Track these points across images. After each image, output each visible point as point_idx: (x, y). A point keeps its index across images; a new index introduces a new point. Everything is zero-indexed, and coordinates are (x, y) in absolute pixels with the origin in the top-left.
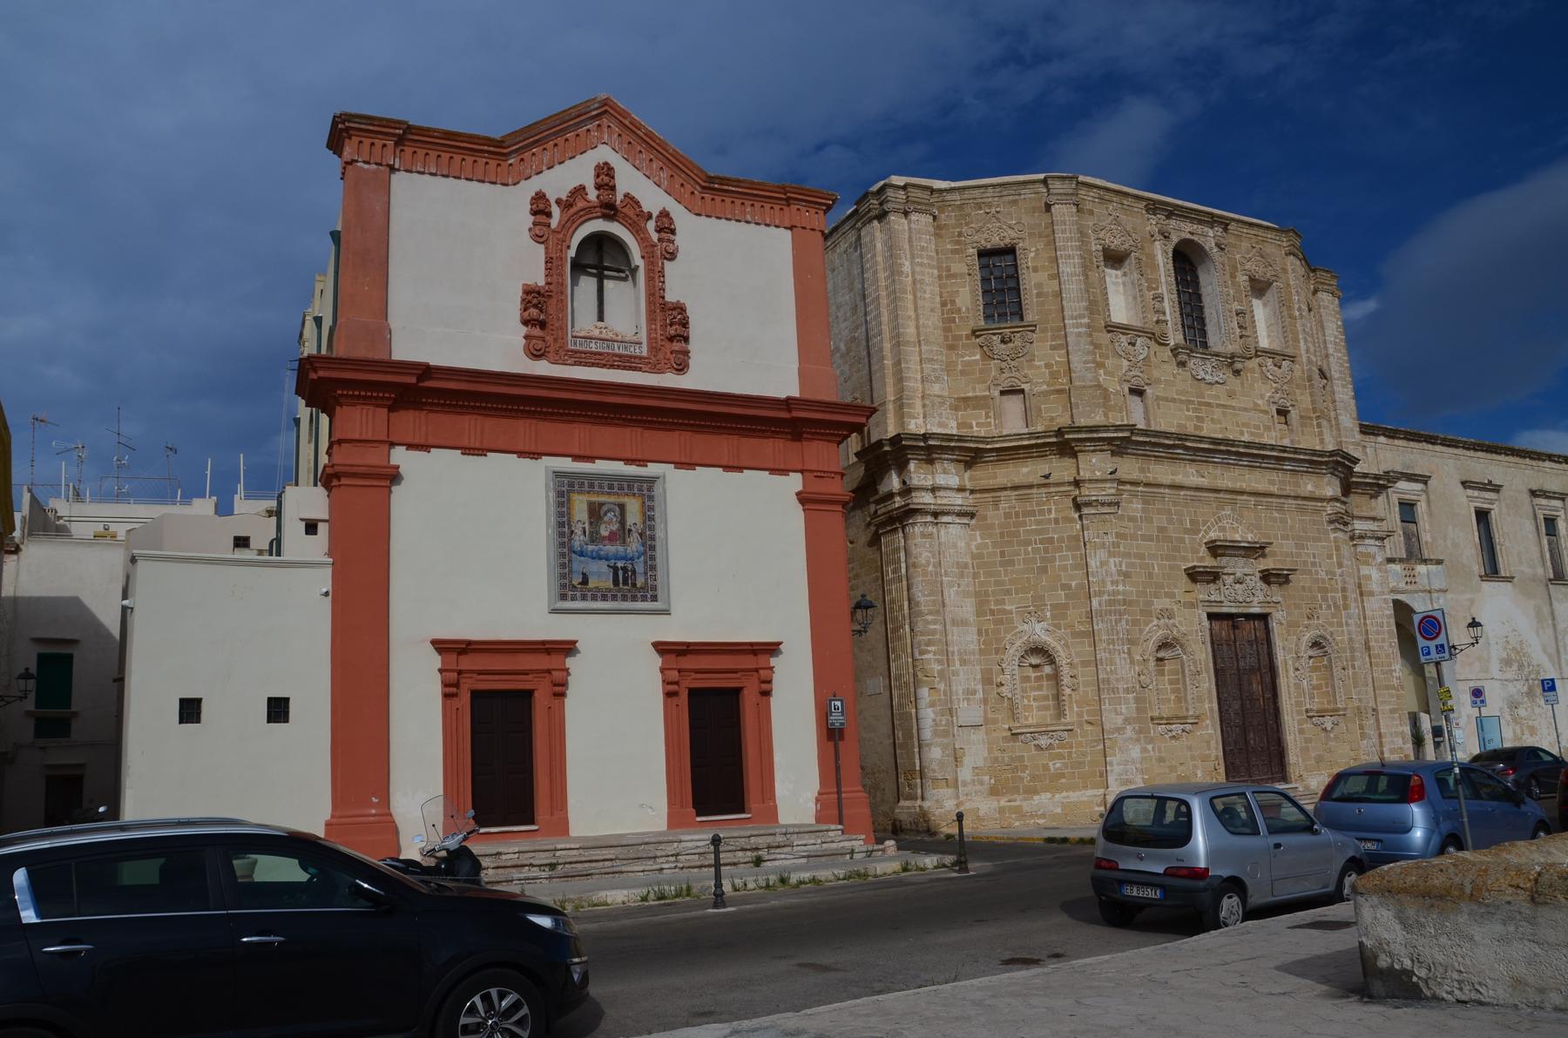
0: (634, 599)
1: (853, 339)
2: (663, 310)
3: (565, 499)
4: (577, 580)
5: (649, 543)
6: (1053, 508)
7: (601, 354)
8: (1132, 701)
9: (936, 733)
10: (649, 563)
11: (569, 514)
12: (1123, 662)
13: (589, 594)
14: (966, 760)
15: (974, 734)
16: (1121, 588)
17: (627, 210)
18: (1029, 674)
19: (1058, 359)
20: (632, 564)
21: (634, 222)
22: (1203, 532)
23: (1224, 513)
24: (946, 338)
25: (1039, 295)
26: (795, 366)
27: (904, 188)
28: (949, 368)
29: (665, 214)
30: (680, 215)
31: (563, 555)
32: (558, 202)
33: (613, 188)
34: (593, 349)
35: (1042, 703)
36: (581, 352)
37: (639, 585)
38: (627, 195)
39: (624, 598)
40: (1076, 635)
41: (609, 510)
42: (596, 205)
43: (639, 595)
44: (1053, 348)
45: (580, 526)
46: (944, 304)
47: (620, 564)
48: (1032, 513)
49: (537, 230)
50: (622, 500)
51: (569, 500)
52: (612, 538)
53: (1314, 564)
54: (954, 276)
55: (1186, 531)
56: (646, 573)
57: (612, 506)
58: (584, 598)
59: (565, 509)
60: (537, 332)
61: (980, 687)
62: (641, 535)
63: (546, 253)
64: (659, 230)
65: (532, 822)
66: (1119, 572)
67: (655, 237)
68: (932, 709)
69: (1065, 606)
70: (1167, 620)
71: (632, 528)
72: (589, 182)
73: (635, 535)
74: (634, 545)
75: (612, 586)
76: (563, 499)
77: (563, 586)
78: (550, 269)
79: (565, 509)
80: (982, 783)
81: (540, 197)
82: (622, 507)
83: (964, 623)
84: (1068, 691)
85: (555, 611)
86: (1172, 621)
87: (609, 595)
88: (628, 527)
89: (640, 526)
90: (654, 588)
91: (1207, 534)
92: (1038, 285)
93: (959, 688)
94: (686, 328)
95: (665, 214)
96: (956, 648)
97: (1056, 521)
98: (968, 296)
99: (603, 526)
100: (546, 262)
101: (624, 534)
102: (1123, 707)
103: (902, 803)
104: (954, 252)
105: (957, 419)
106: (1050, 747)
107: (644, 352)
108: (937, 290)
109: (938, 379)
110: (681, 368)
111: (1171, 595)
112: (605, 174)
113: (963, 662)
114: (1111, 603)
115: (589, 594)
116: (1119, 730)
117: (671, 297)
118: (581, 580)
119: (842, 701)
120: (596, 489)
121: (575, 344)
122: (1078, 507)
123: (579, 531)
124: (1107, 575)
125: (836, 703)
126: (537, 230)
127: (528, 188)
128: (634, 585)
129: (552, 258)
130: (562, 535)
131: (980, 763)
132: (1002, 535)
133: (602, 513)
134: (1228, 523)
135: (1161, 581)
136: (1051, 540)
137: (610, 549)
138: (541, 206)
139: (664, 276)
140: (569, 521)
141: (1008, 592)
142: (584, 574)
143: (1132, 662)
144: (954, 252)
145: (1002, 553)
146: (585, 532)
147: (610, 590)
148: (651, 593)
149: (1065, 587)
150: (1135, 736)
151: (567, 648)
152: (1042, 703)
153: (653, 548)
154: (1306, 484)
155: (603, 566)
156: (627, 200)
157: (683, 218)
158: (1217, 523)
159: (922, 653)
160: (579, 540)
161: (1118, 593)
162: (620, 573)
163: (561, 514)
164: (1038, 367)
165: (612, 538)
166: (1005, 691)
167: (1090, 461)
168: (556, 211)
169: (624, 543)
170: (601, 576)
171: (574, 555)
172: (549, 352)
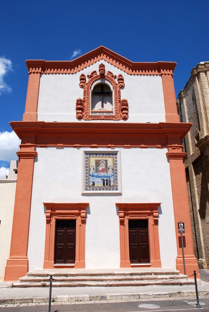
0: (110, 190)
2: (120, 102)
3: (88, 159)
4: (91, 184)
5: (115, 172)
7: (100, 116)
10: (115, 178)
11: (89, 164)
13: (95, 188)
21: (111, 78)
26: (164, 115)
27: (204, 65)
31: (87, 176)
32: (88, 76)
33: (104, 70)
36: (94, 116)
37: (111, 185)
39: (107, 189)
41: (102, 162)
43: (111, 188)
45: (93, 167)
47: (105, 179)
49: (82, 84)
50: (106, 159)
51: (89, 160)
52: (103, 171)
56: (114, 181)
58: (93, 190)
60: (80, 111)
62: (112, 169)
63: (84, 90)
64: (119, 80)
71: (110, 167)
73: (111, 169)
74: (110, 173)
75: (102, 186)
77: (86, 186)
78: (85, 94)
81: (83, 75)
82: (106, 161)
85: (83, 194)
89: (112, 167)
90: (117, 186)
94: (127, 106)
95: (120, 76)
99: (100, 167)
100: (84, 92)
101: (107, 169)
103: (200, 259)
107: (114, 114)
110: (125, 119)
112: (102, 66)
115: (95, 188)
117: (122, 98)
119: (183, 223)
123: (92, 169)
125: (181, 224)
126: (82, 84)
128: (110, 185)
129: (85, 91)
130: (87, 170)
133: (100, 163)
137: (102, 174)
138: (83, 77)
139: (120, 93)
140: (89, 166)
142: (93, 182)
146: (94, 169)
147: (102, 187)
148: (116, 188)
156: (109, 73)
157: (126, 76)
160: (92, 171)
162: (105, 182)
163: (87, 164)
165: (103, 171)
168: (87, 80)
170: (99, 183)
171: (90, 176)
172: (84, 117)
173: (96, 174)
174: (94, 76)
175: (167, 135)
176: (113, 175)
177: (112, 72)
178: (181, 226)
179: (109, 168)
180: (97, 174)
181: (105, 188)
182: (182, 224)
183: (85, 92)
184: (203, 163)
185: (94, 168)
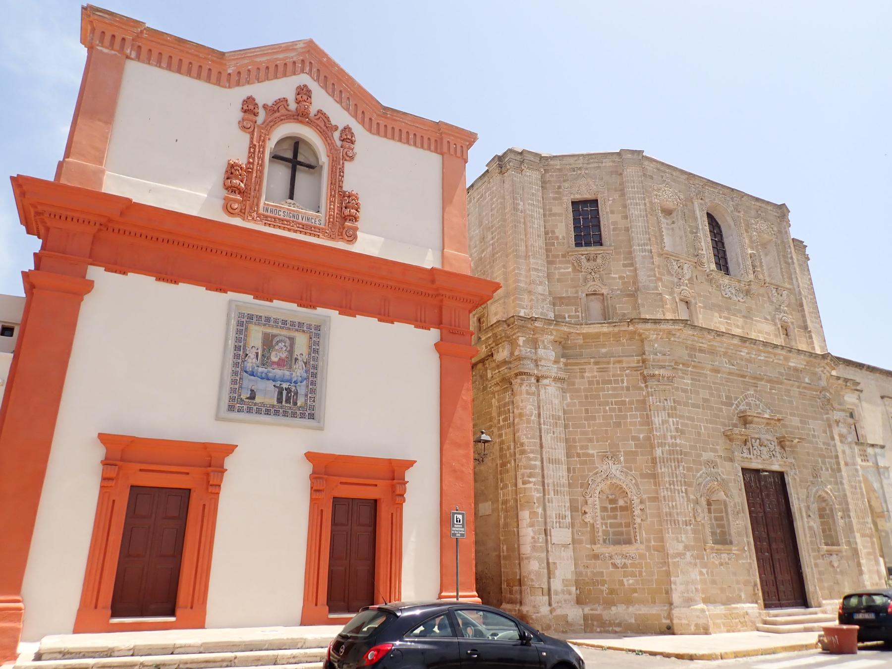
1: (481, 259)
3: (244, 328)
4: (245, 395)
6: (625, 379)
8: (690, 532)
9: (534, 548)
10: (310, 387)
12: (682, 500)
13: (255, 408)
14: (557, 573)
15: (564, 551)
16: (678, 441)
17: (323, 124)
18: (606, 506)
19: (628, 273)
20: (295, 387)
22: (735, 405)
23: (749, 392)
24: (547, 256)
25: (614, 230)
28: (549, 276)
29: (347, 129)
30: (358, 130)
31: (235, 373)
32: (265, 107)
34: (282, 217)
35: (617, 529)
37: (299, 404)
38: (319, 111)
39: (285, 414)
40: (643, 476)
42: (294, 113)
43: (298, 412)
44: (625, 266)
45: (254, 350)
46: (546, 233)
47: (285, 385)
48: (610, 382)
51: (246, 329)
52: (281, 363)
53: (814, 436)
54: (555, 215)
55: (723, 403)
56: (306, 395)
57: (284, 338)
58: (249, 410)
59: (242, 336)
61: (568, 513)
62: (305, 363)
65: (172, 613)
66: (677, 430)
67: (339, 143)
68: (531, 528)
69: (635, 453)
70: (712, 469)
71: (299, 357)
72: (291, 97)
73: (300, 363)
74: (299, 371)
75: (275, 403)
76: (242, 328)
77: (232, 399)
79: (242, 336)
80: (570, 593)
82: (292, 340)
83: (557, 462)
84: (638, 520)
86: (716, 470)
87: (272, 410)
88: (295, 356)
89: (305, 357)
90: (313, 408)
91: (738, 407)
92: (614, 223)
93: (552, 513)
95: (347, 129)
96: (551, 481)
97: (628, 388)
98: (564, 228)
99: (273, 354)
102: (683, 536)
104: (555, 199)
105: (554, 312)
106: (625, 566)
108: (542, 223)
109: (541, 283)
111: (714, 450)
112: (303, 93)
113: (556, 492)
114: (671, 452)
115: (255, 408)
116: (681, 555)
117: (347, 187)
118: (249, 396)
119: (463, 514)
120: (272, 323)
121: (267, 210)
122: (645, 379)
123: (252, 355)
124: (667, 430)
127: (241, 93)
128: (295, 404)
130: (236, 356)
131: (569, 576)
132: (586, 397)
133: (274, 343)
134: (752, 400)
135: (707, 439)
136: (624, 403)
137: (278, 372)
138: (251, 107)
139: (343, 172)
140: (245, 346)
141: (591, 440)
142: (252, 391)
143: (688, 500)
144: (555, 199)
145: (587, 411)
147: (273, 406)
149: (635, 438)
150: (693, 561)
151: (229, 449)
152: (617, 529)
153: (314, 375)
154: (804, 378)
155: (270, 385)
158: (745, 400)
159: (524, 483)
160: (251, 362)
161: (676, 445)
162: (285, 393)
164: (615, 278)
165: (281, 363)
166: (588, 518)
167: (654, 346)
169: (291, 368)
170: (267, 394)
171: (245, 374)
173: (261, 369)
174: (283, 111)
175: (442, 301)
176: (306, 379)
177: (328, 114)
178: (457, 521)
179: (296, 359)
180: (265, 370)
181: (281, 411)
182: (460, 517)
183: (252, 146)
184: (489, 375)
185: (257, 354)
